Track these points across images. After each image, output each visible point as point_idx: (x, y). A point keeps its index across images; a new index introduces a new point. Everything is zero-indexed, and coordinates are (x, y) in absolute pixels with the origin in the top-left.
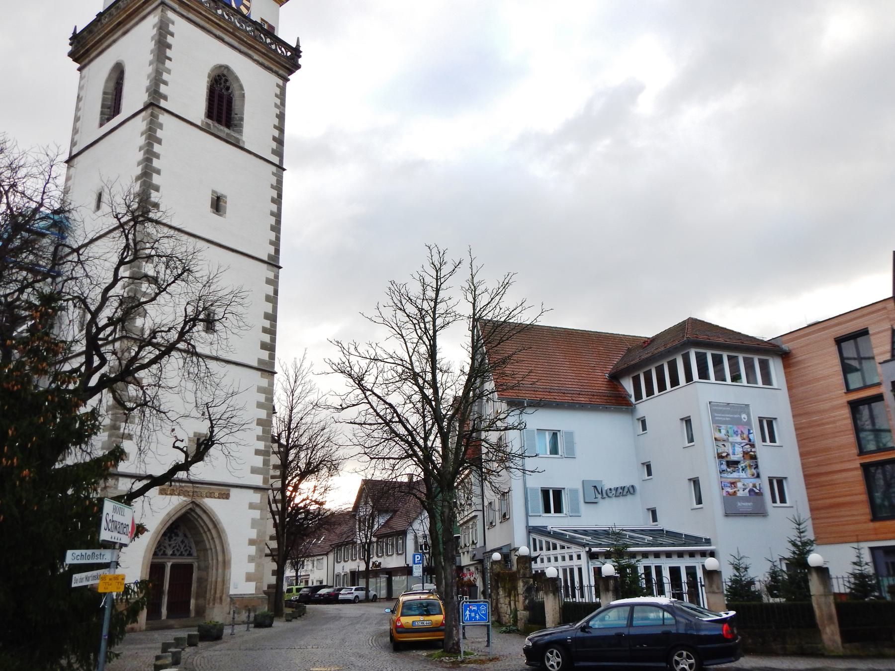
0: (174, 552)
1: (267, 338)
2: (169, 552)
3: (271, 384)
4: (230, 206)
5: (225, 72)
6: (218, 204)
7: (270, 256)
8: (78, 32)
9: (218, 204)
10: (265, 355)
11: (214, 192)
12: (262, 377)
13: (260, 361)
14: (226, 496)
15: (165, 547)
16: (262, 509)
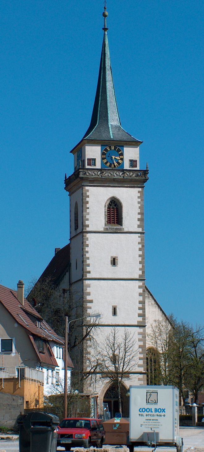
0: (114, 397)
1: (141, 312)
2: (112, 396)
3: (145, 331)
4: (119, 261)
5: (113, 199)
6: (114, 262)
7: (140, 275)
8: (67, 177)
9: (114, 262)
10: (140, 319)
11: (111, 257)
12: (140, 328)
13: (138, 322)
14: (128, 377)
15: (111, 395)
16: (144, 381)
